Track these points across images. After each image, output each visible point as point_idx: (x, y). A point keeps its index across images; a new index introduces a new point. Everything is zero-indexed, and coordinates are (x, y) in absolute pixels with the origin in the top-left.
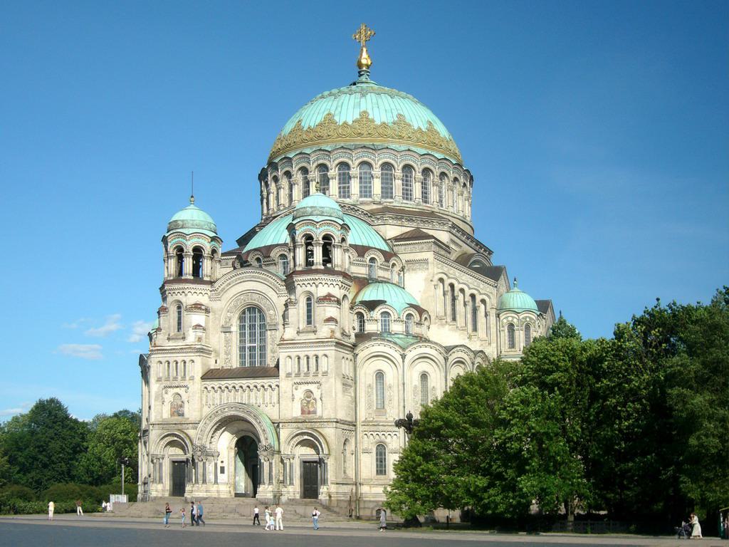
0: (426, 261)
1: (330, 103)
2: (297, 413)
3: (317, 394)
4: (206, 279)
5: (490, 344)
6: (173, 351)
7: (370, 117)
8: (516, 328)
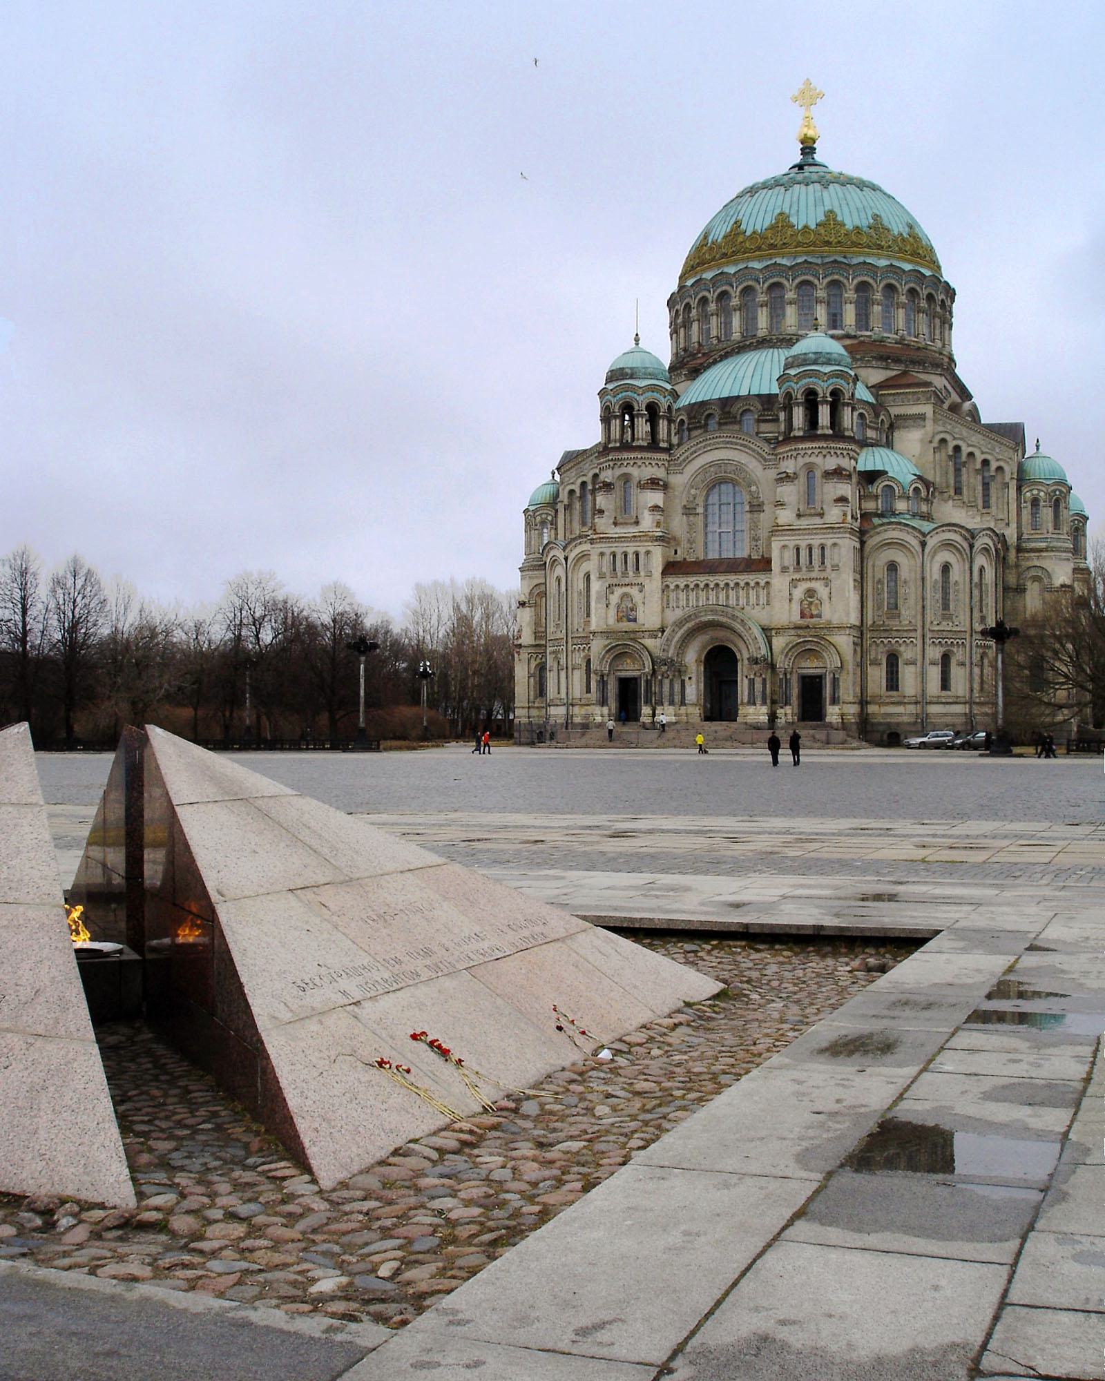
0: (922, 417)
1: (781, 197)
2: (796, 618)
3: (822, 591)
4: (662, 445)
5: (1008, 524)
6: (620, 539)
7: (839, 218)
8: (1042, 503)
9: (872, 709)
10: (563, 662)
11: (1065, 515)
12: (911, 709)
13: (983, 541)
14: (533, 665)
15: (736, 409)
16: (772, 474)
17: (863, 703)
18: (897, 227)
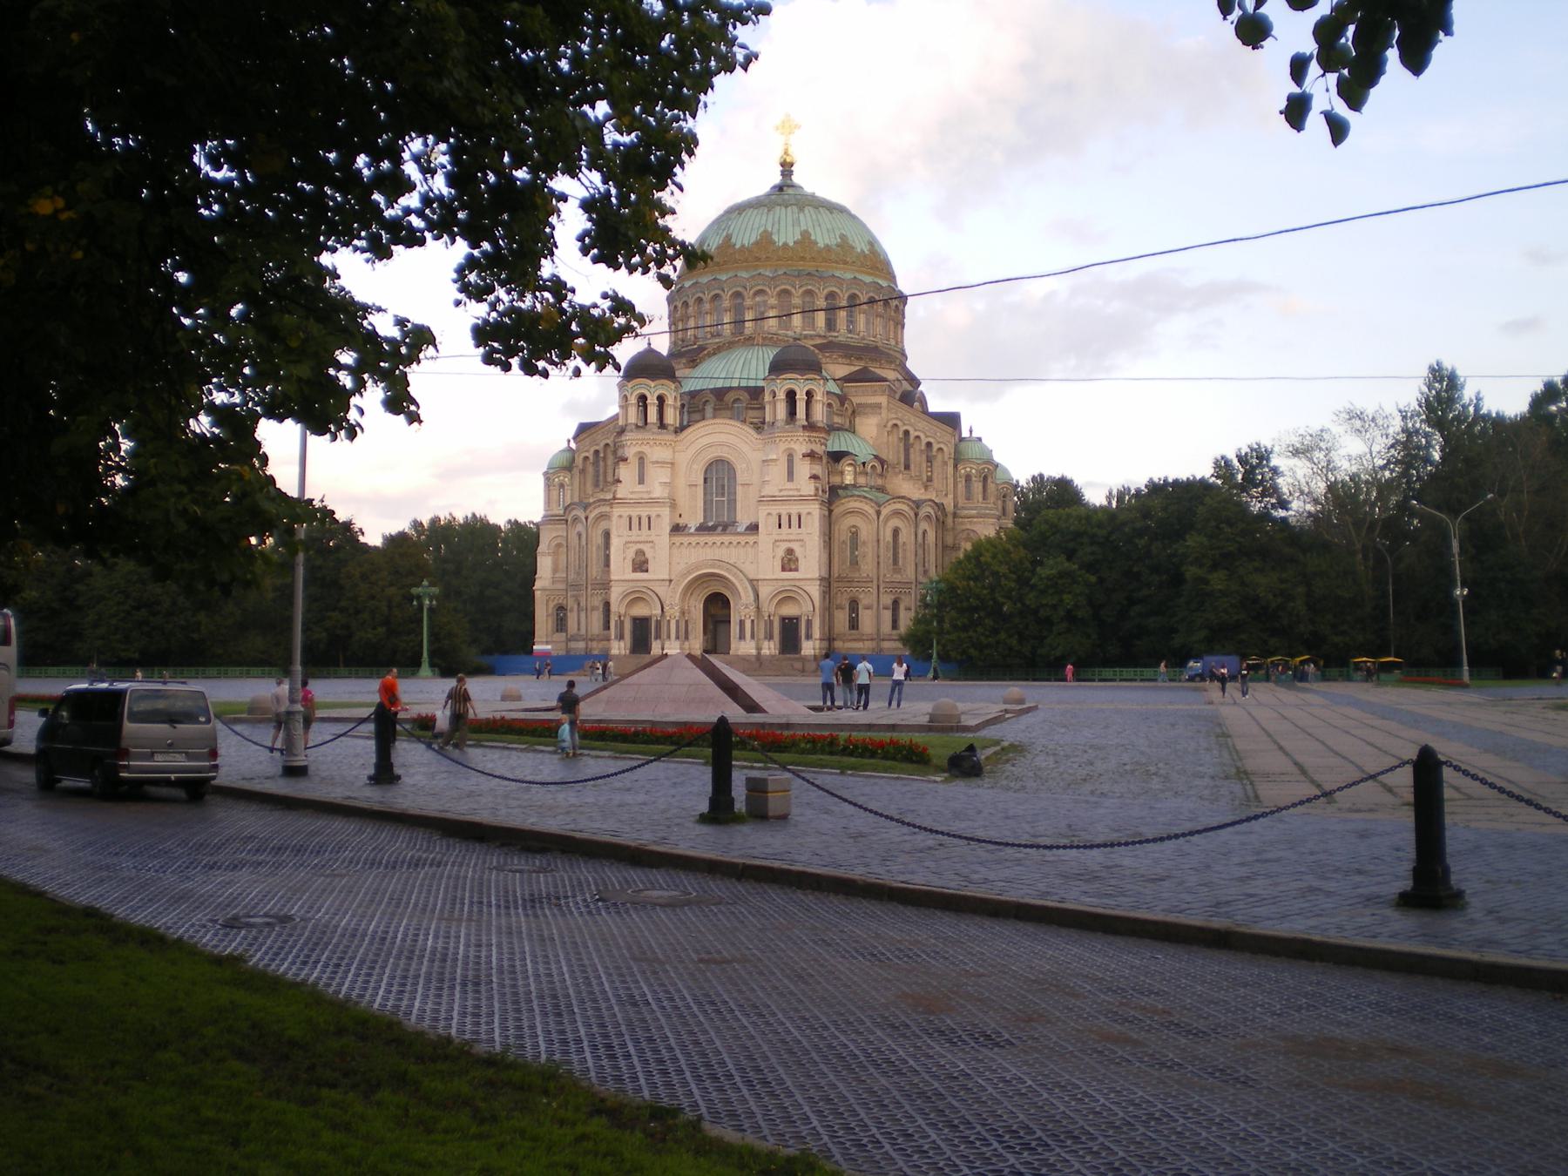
9: (838, 644)
10: (583, 604)
11: (991, 487)
12: (869, 644)
13: (927, 509)
14: (551, 605)
15: (730, 397)
16: (760, 456)
17: (829, 638)
18: (861, 246)
